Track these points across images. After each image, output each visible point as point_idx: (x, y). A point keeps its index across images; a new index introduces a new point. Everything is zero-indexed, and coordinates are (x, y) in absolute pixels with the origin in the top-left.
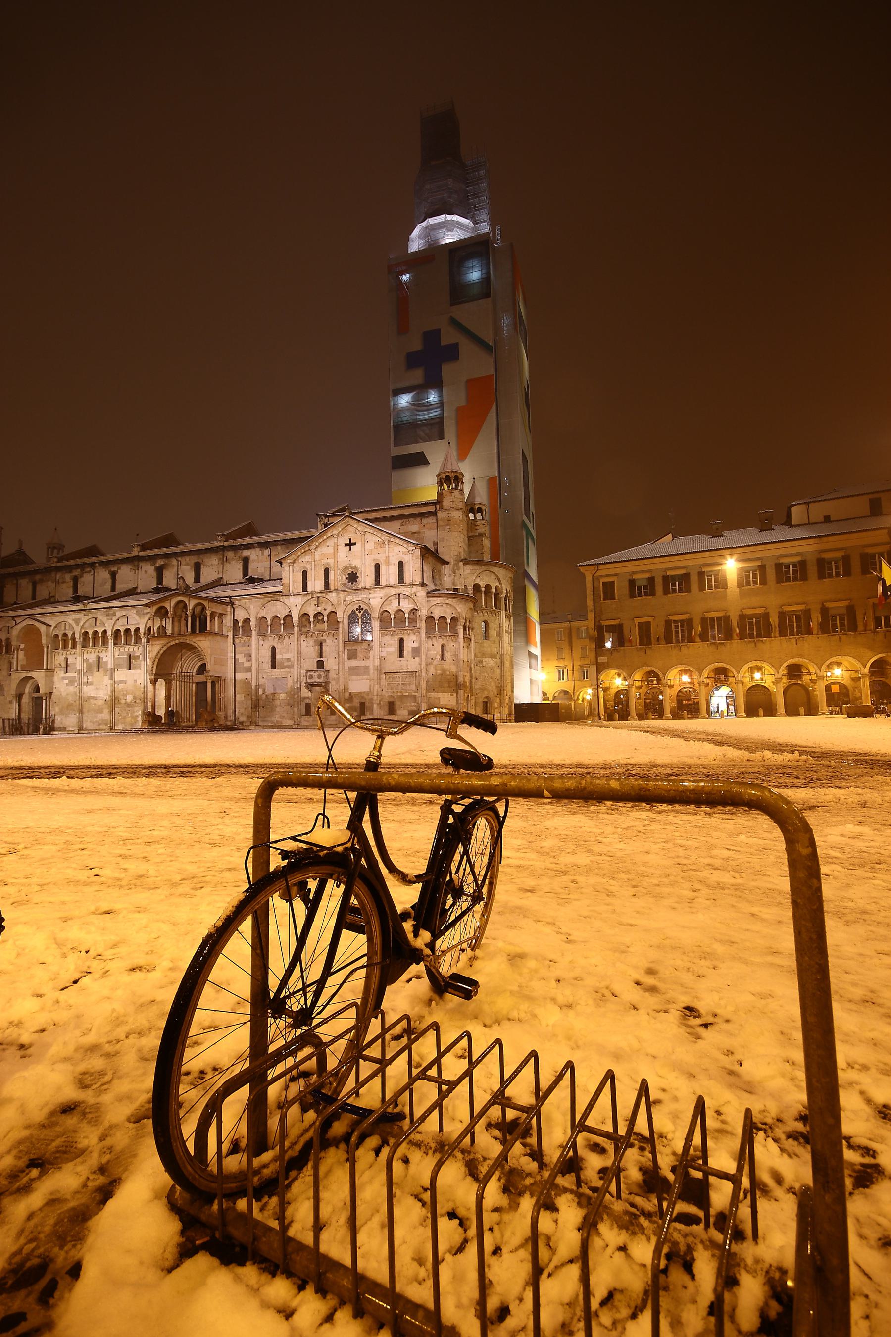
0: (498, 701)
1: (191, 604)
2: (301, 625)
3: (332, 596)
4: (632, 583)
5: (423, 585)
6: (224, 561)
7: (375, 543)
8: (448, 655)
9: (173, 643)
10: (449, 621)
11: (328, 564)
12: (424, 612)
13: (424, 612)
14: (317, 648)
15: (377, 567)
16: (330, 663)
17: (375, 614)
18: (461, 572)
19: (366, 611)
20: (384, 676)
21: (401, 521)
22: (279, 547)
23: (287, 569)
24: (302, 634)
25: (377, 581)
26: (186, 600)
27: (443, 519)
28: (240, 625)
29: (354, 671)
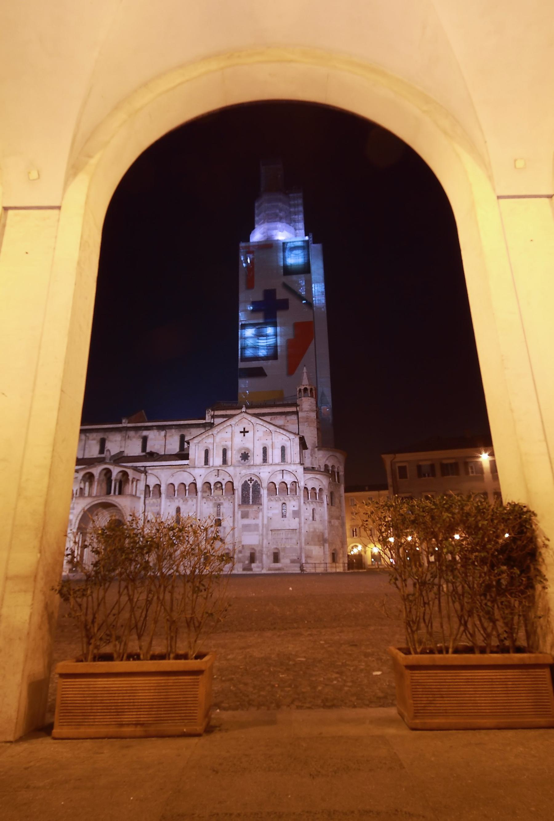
0: (342, 552)
1: (116, 471)
2: (203, 491)
3: (230, 470)
4: (419, 467)
5: (302, 464)
6: (126, 438)
7: (264, 432)
8: (317, 517)
9: (96, 502)
10: (318, 491)
11: (226, 445)
12: (302, 484)
13: (302, 484)
14: (216, 509)
15: (265, 450)
16: (227, 523)
17: (265, 485)
18: (316, 456)
19: (256, 481)
20: (270, 532)
21: (270, 417)
22: (173, 430)
23: (194, 447)
24: (203, 497)
25: (265, 460)
26: (111, 467)
27: (303, 418)
28: (151, 489)
29: (246, 527)
